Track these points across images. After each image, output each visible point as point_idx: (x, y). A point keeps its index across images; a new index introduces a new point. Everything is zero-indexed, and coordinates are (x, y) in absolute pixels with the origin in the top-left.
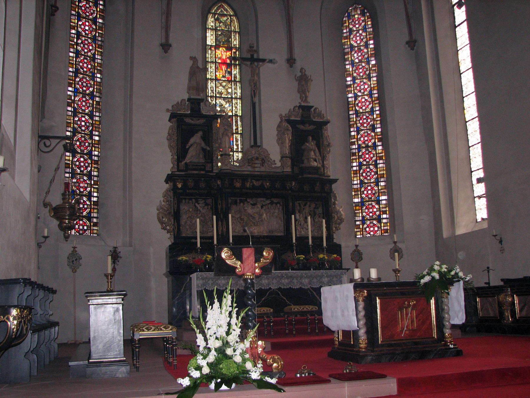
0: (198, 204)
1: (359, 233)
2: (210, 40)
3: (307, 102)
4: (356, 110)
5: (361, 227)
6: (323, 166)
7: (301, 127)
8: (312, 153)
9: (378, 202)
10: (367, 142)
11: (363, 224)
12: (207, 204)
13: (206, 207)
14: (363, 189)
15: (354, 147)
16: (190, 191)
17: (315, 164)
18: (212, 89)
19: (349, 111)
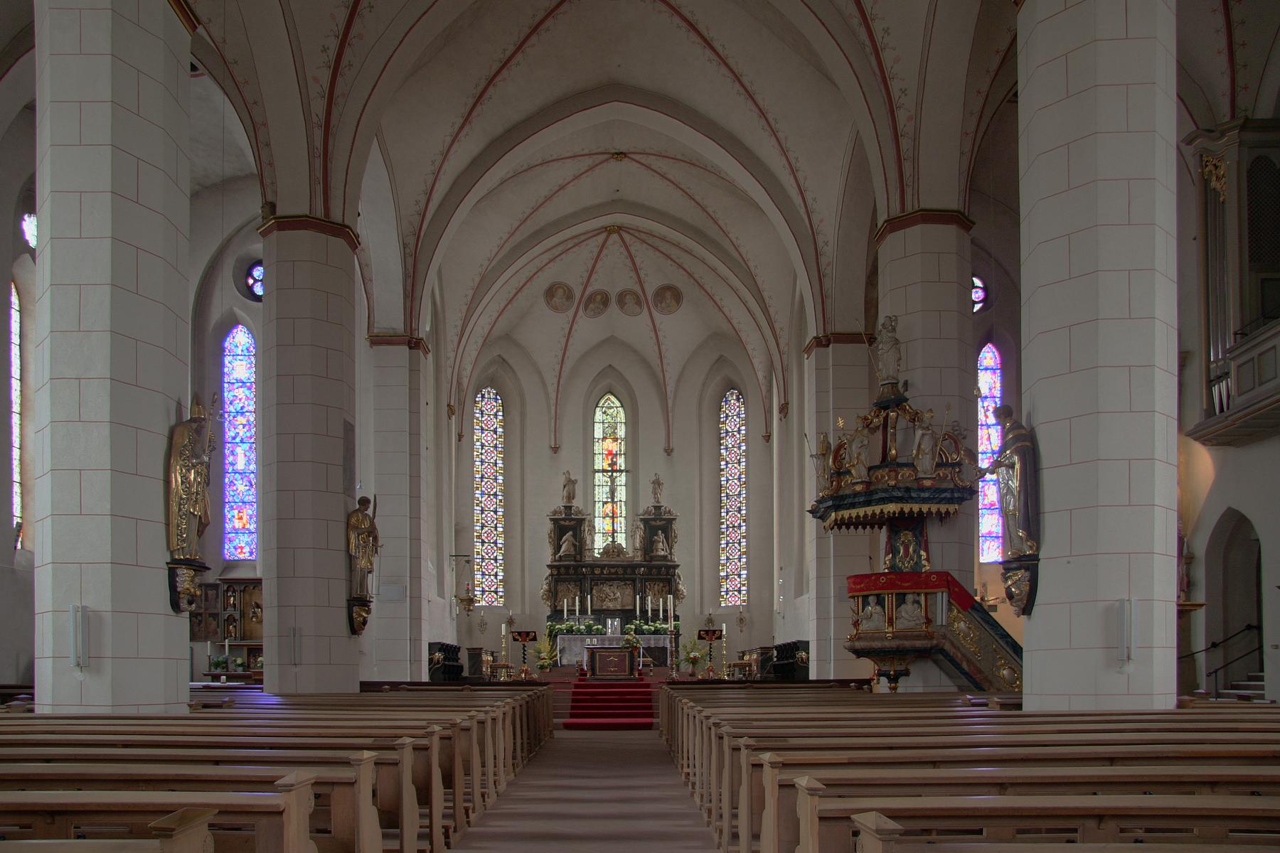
2: (598, 433)
9: (739, 576)
17: (662, 553)
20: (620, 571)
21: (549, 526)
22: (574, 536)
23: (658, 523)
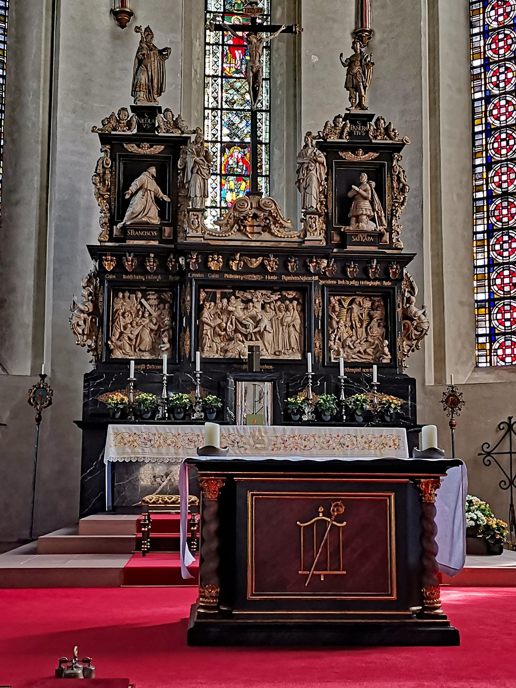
0: (147, 300)
1: (483, 359)
3: (363, 108)
4: (487, 124)
5: (488, 346)
6: (390, 229)
7: (349, 156)
8: (367, 204)
10: (505, 185)
11: (492, 341)
12: (161, 301)
13: (161, 306)
14: (493, 275)
15: (480, 195)
16: (130, 277)
17: (370, 226)
18: (215, 94)
19: (474, 126)
20: (272, 264)
21: (96, 151)
22: (160, 180)
23: (362, 157)
